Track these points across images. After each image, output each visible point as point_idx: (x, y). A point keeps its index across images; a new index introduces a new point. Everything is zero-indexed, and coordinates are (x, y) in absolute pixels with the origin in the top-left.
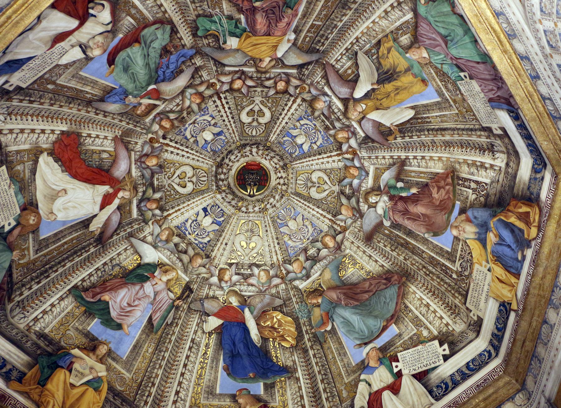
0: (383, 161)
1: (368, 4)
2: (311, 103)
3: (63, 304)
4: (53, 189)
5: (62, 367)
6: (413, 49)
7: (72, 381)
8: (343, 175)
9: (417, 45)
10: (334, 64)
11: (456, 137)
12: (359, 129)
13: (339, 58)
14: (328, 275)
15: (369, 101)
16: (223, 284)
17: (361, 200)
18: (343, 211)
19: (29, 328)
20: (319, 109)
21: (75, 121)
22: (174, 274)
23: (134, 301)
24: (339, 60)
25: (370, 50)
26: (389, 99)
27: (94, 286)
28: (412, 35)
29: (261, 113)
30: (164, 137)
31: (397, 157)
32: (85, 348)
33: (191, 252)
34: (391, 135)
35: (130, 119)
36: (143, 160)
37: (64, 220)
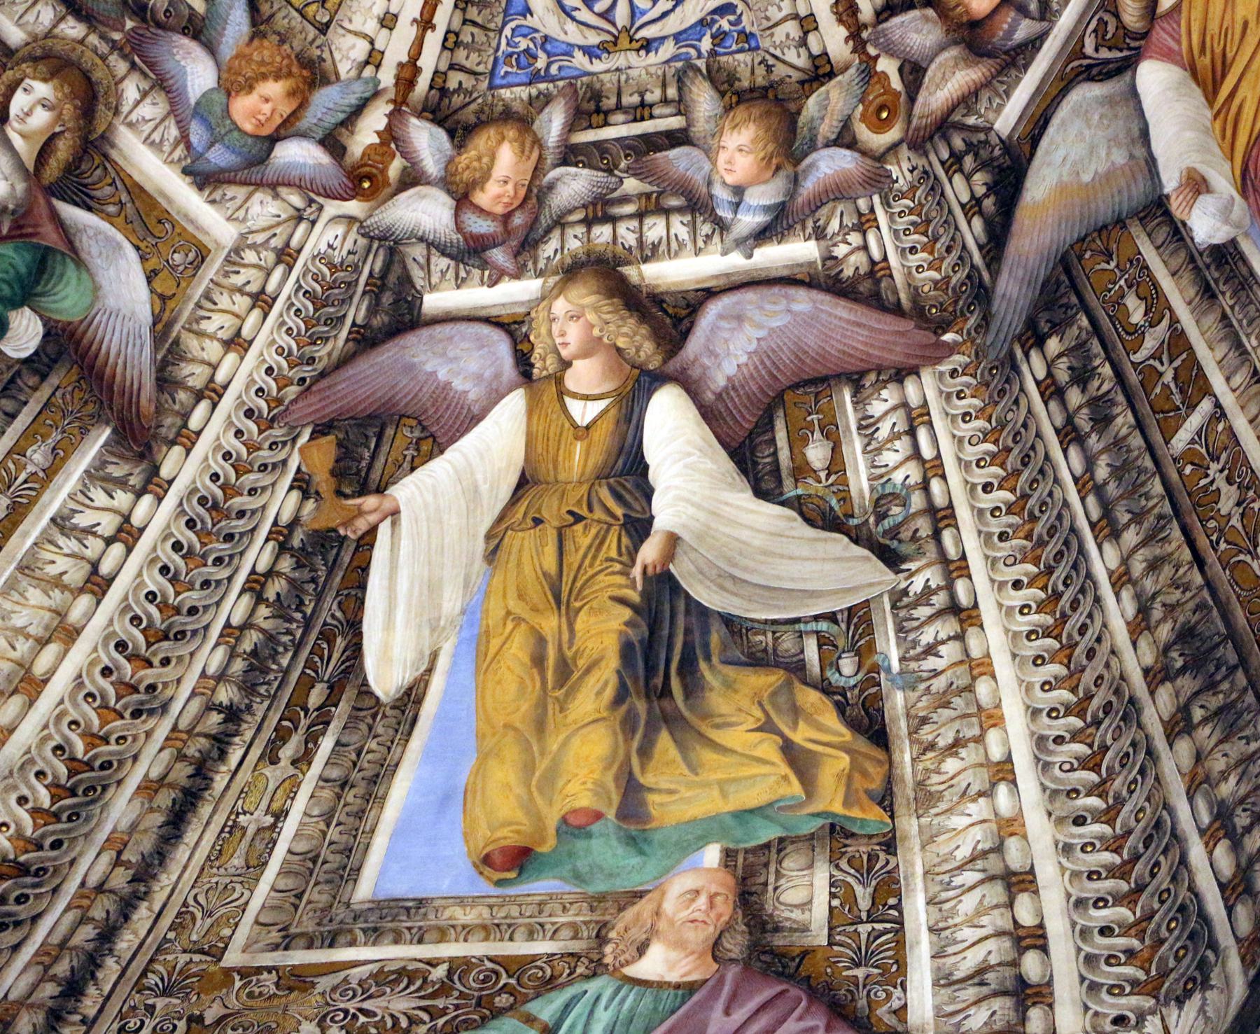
0: (217, 323)
1: (1120, 802)
6: (725, 908)
8: (281, 23)
9: (735, 946)
10: (911, 387)
13: (923, 435)
15: (596, 458)
20: (718, 133)
24: (912, 432)
25: (864, 650)
26: (536, 592)
28: (806, 953)
31: (195, 422)
34: (338, 473)
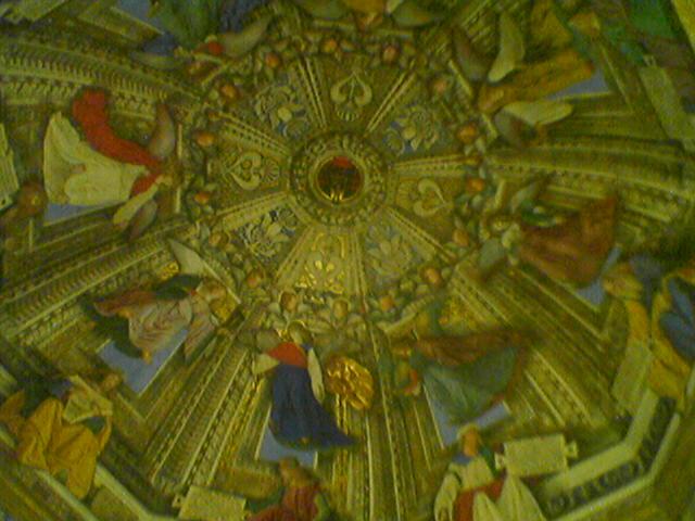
2: (429, 82)
3: (66, 315)
4: (68, 163)
5: (54, 396)
7: (65, 416)
10: (466, 28)
11: (629, 151)
12: (490, 126)
14: (424, 320)
16: (286, 315)
17: (481, 225)
18: (456, 237)
19: (18, 340)
21: (103, 74)
22: (222, 292)
23: (163, 322)
27: (111, 296)
29: (358, 88)
30: (226, 109)
32: (89, 377)
33: (248, 267)
35: (179, 80)
36: (194, 137)
37: (79, 203)
